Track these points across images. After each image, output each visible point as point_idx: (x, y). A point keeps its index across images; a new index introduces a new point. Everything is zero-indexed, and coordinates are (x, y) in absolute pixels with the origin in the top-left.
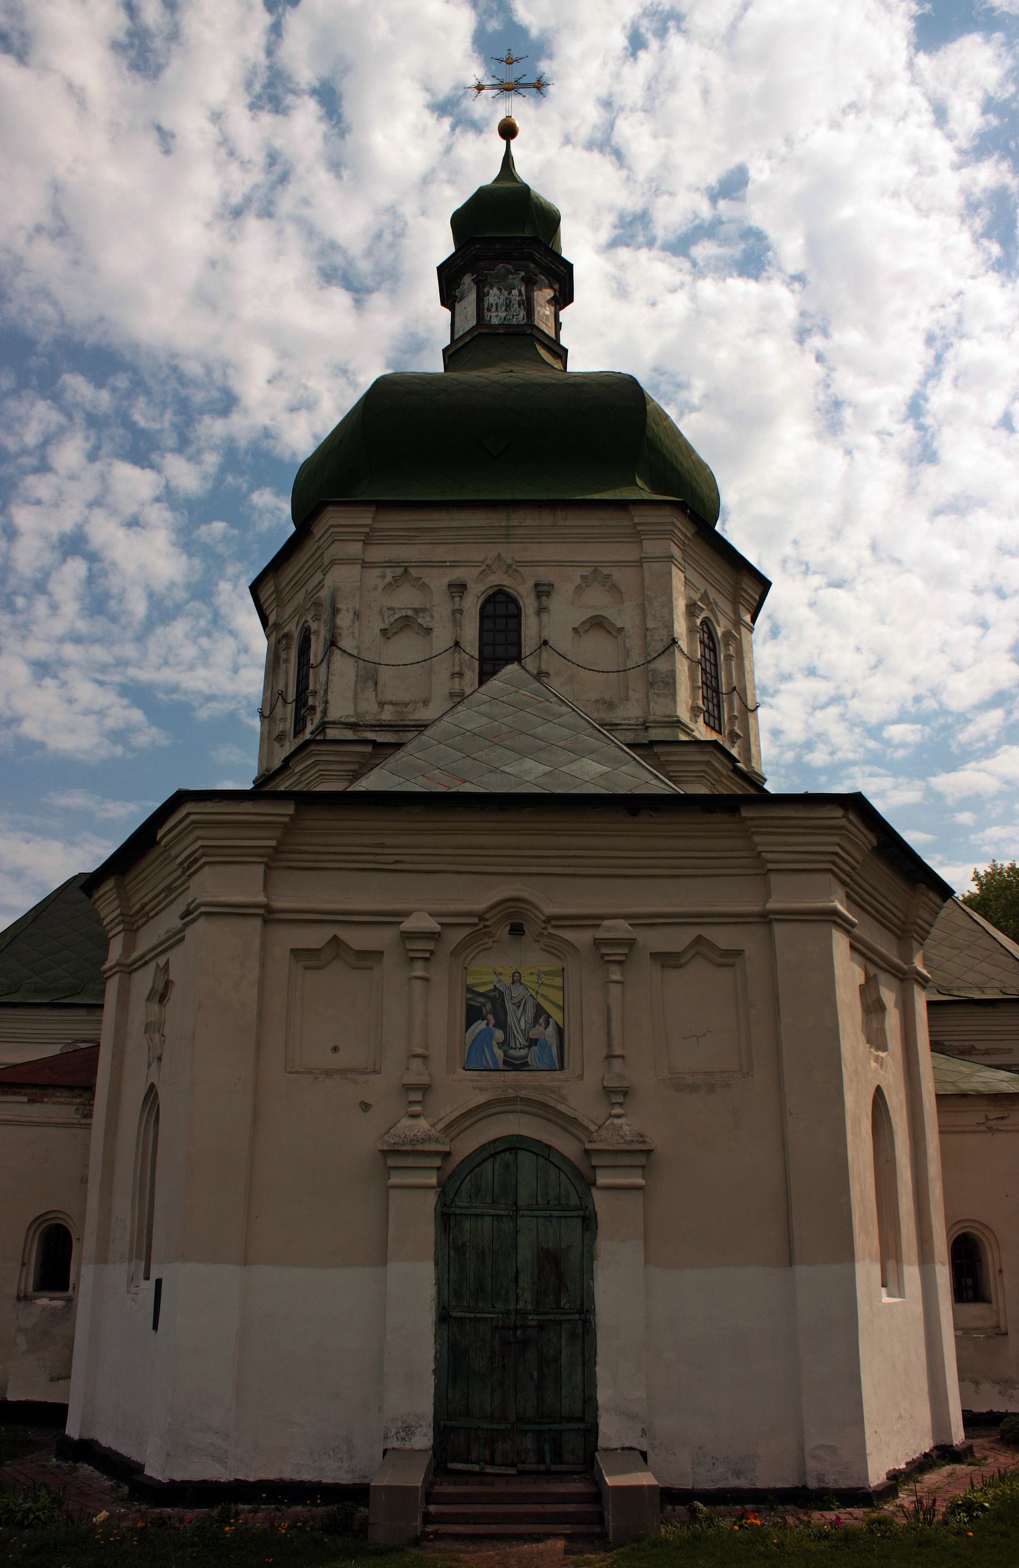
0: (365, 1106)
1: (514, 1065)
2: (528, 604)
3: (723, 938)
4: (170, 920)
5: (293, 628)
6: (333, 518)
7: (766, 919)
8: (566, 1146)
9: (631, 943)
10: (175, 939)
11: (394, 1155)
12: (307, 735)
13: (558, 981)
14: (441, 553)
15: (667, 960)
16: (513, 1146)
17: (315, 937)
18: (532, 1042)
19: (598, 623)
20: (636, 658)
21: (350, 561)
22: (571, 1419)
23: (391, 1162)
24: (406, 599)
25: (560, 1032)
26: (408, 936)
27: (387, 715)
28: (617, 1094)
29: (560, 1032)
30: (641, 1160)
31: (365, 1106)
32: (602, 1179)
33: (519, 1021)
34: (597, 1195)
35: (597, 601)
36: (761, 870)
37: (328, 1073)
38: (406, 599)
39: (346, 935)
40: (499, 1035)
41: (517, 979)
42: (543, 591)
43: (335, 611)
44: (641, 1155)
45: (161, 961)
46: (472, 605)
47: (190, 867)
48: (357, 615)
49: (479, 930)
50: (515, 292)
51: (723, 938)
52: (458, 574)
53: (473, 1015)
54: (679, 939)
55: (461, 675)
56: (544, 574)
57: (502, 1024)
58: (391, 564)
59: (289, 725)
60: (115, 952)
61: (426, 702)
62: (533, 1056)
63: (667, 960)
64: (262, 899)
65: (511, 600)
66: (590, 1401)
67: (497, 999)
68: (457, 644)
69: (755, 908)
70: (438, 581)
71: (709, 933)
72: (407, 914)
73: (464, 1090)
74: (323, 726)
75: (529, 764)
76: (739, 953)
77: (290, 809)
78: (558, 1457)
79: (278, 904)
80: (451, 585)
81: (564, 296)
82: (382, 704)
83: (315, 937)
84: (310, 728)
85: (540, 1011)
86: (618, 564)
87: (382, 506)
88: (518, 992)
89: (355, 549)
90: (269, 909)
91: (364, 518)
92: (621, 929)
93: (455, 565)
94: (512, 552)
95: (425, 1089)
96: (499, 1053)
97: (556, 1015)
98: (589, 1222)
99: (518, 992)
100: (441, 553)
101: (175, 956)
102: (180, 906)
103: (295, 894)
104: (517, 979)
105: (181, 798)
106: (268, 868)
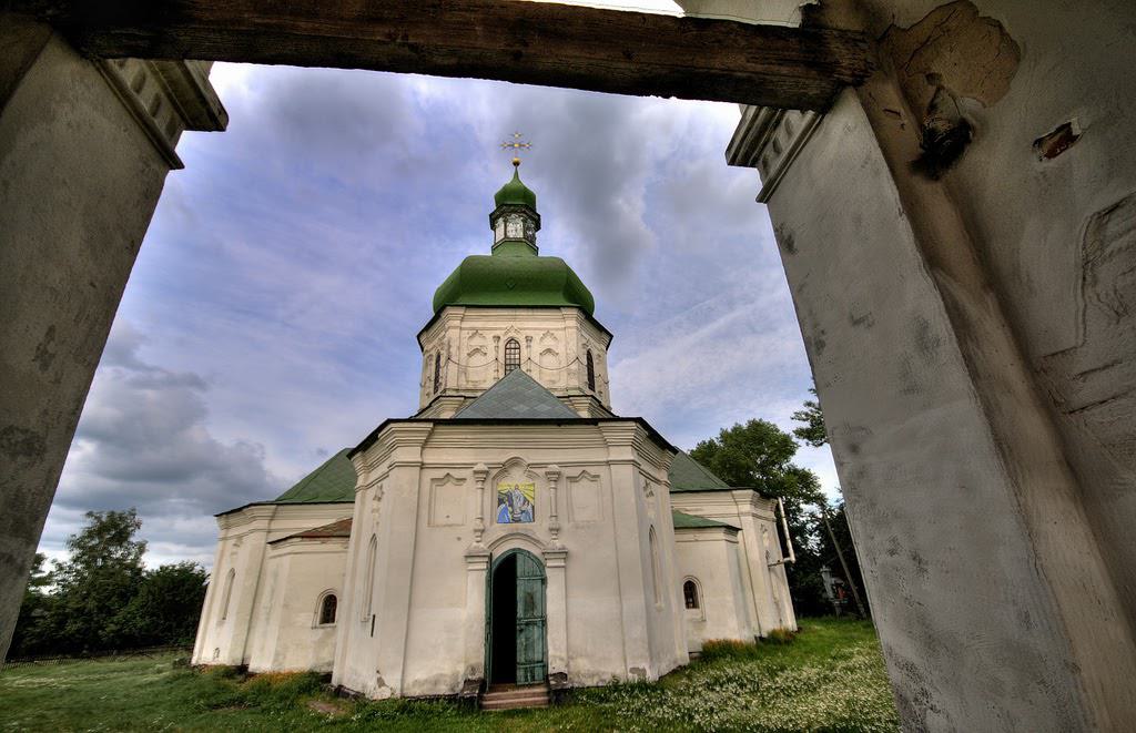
0: (459, 539)
2: (523, 344)
3: (592, 470)
4: (383, 468)
5: (434, 353)
6: (450, 311)
7: (608, 463)
8: (536, 551)
9: (559, 474)
10: (385, 476)
12: (439, 394)
13: (532, 488)
14: (491, 325)
15: (572, 479)
17: (440, 474)
18: (523, 512)
19: (549, 351)
20: (564, 364)
21: (455, 327)
22: (538, 662)
23: (469, 560)
24: (477, 342)
25: (533, 507)
26: (475, 472)
27: (470, 386)
28: (556, 531)
29: (533, 507)
30: (564, 556)
31: (459, 539)
32: (549, 563)
33: (518, 504)
34: (547, 570)
35: (549, 343)
36: (606, 445)
38: (477, 342)
39: (452, 472)
40: (510, 509)
41: (517, 488)
42: (529, 339)
43: (450, 347)
44: (564, 554)
45: (379, 484)
46: (502, 344)
47: (392, 448)
48: (459, 348)
49: (504, 468)
51: (592, 470)
52: (498, 333)
53: (501, 501)
54: (575, 472)
56: (529, 333)
57: (511, 505)
59: (432, 390)
60: (360, 482)
61: (485, 381)
62: (523, 517)
63: (572, 479)
64: (420, 460)
66: (545, 653)
69: (605, 459)
70: (490, 335)
71: (588, 469)
72: (476, 464)
73: (499, 530)
74: (445, 390)
75: (521, 406)
76: (598, 476)
77: (431, 425)
78: (533, 677)
79: (425, 461)
80: (494, 337)
81: (538, 227)
82: (468, 382)
83: (440, 474)
84: (440, 391)
85: (525, 500)
86: (557, 329)
87: (468, 307)
88: (517, 492)
89: (457, 323)
90: (423, 464)
91: (461, 311)
92: (555, 468)
94: (517, 325)
95: (483, 531)
96: (510, 516)
98: (544, 581)
99: (517, 492)
100: (491, 325)
101: (384, 482)
102: (387, 463)
103: (432, 457)
104: (517, 488)
105: (389, 421)
106: (423, 448)
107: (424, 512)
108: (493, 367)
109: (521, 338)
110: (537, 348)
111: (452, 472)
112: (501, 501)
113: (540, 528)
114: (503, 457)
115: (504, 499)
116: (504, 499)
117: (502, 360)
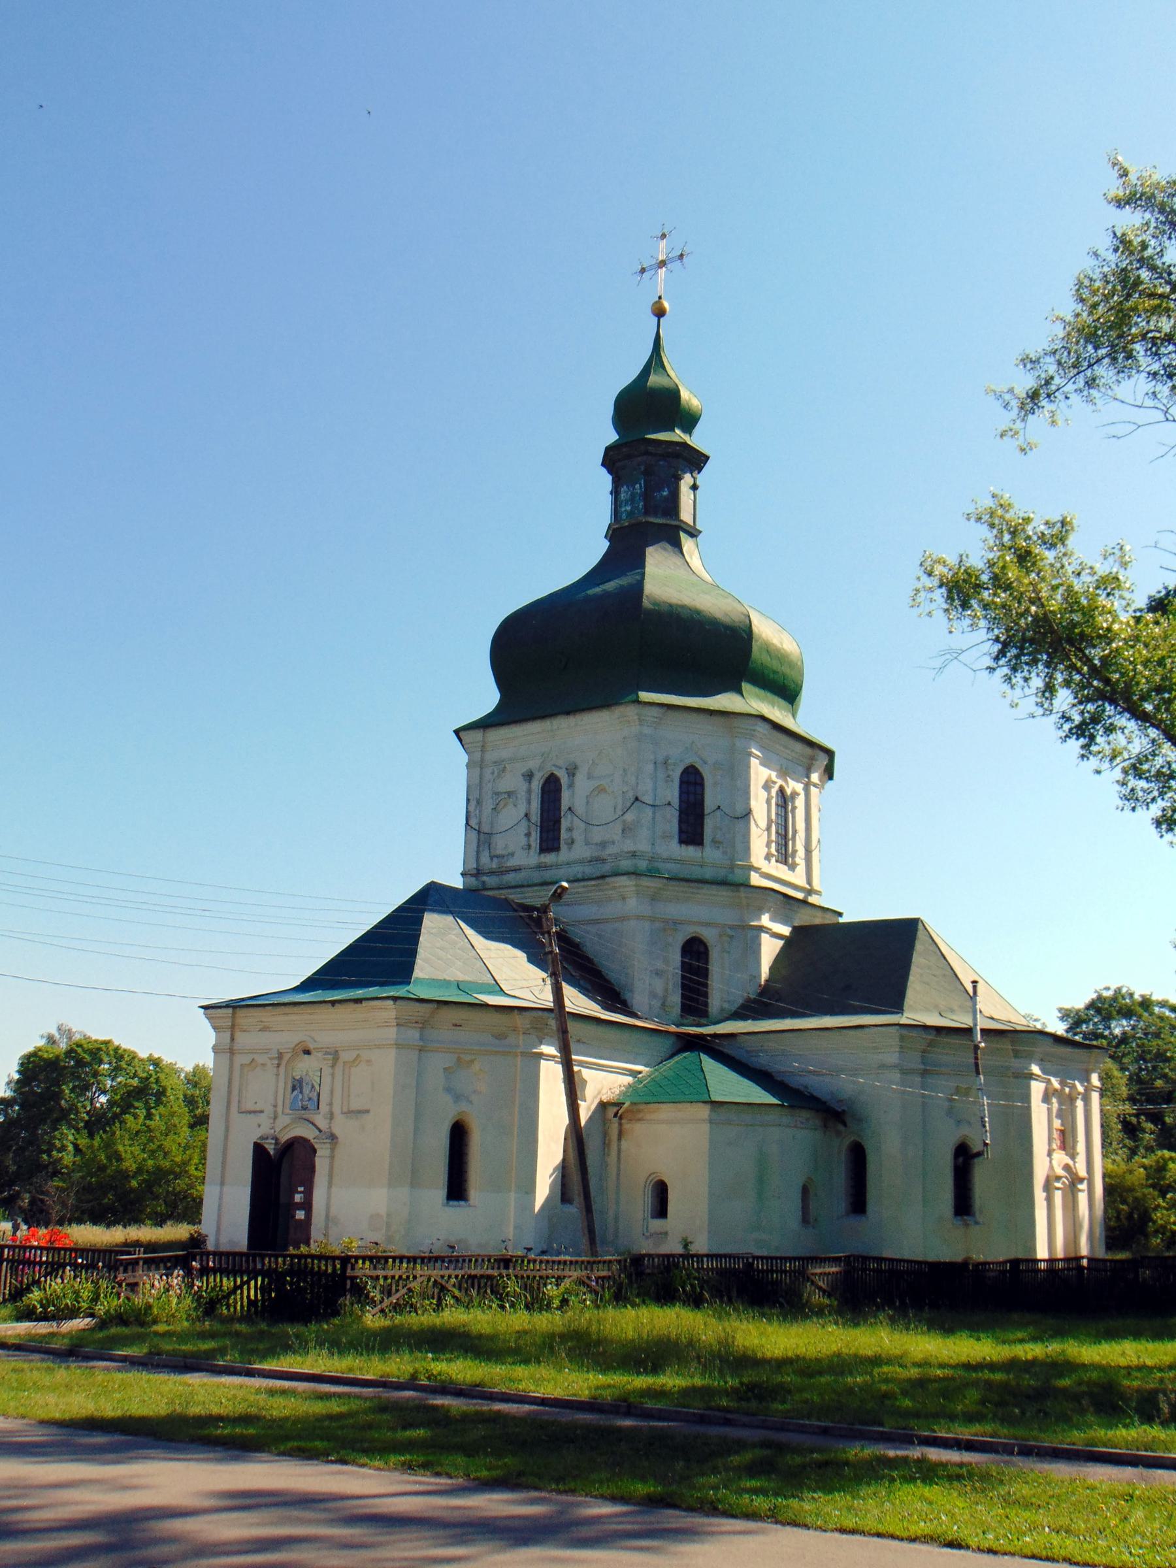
1: (305, 1108)
2: (564, 780)
18: (310, 1099)
25: (319, 1095)
33: (306, 1090)
37: (250, 1112)
42: (572, 772)
46: (537, 785)
50: (637, 486)
57: (301, 1092)
61: (512, 854)
67: (300, 1081)
68: (526, 815)
73: (283, 1121)
82: (492, 858)
97: (317, 1087)
108: (523, 828)
111: (256, 1057)
115: (297, 1085)
116: (297, 1085)
117: (536, 817)
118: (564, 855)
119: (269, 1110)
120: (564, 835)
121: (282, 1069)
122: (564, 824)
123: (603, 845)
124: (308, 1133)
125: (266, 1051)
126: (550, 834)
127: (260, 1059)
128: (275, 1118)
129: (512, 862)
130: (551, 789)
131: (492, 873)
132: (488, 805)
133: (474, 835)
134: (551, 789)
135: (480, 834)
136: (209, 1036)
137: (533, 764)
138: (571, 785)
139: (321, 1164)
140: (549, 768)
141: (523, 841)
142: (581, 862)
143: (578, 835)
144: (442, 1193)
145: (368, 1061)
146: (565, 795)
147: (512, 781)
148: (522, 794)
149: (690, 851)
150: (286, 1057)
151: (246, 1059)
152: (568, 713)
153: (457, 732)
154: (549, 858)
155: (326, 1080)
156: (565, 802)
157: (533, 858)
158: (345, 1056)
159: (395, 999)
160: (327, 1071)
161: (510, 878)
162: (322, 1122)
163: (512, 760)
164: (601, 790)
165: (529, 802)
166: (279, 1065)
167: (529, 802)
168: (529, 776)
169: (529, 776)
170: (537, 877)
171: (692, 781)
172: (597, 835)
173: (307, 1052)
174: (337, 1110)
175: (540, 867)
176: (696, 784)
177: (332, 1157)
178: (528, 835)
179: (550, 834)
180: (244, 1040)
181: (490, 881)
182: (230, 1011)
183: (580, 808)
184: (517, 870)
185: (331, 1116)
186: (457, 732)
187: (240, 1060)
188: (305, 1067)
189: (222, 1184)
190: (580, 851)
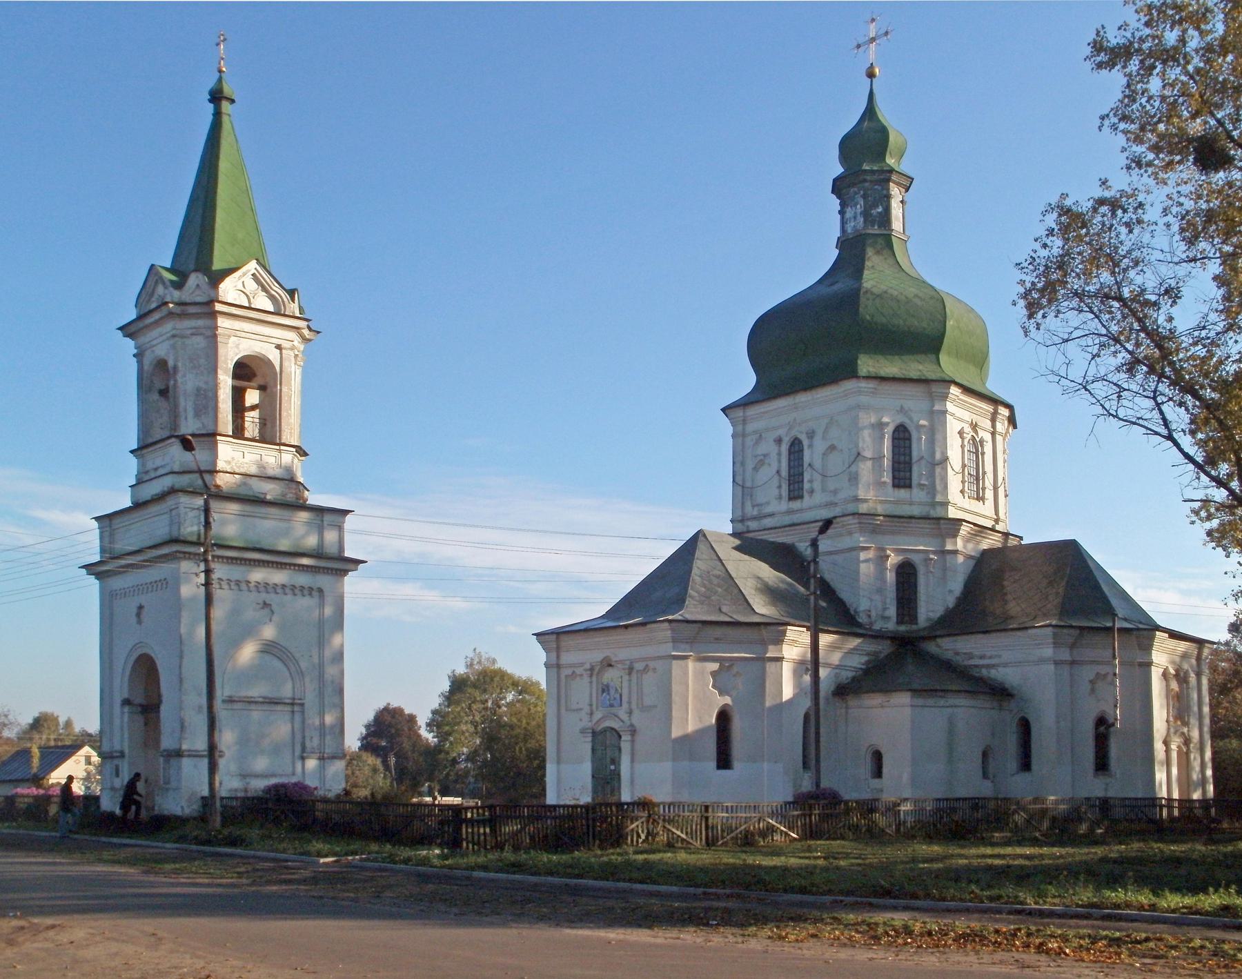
1: (612, 706)
2: (806, 443)
11: (583, 731)
16: (605, 730)
24: (763, 449)
27: (755, 513)
33: (612, 692)
38: (763, 449)
42: (811, 435)
46: (785, 448)
51: (652, 664)
53: (603, 691)
55: (780, 487)
58: (755, 432)
65: (800, 442)
67: (607, 686)
73: (598, 715)
82: (753, 506)
93: (775, 428)
98: (620, 750)
107: (563, 701)
108: (775, 482)
109: (803, 437)
110: (820, 445)
112: (603, 691)
113: (622, 713)
114: (597, 656)
116: (605, 689)
117: (784, 473)
118: (807, 501)
119: (587, 709)
120: (806, 486)
121: (594, 679)
122: (807, 477)
123: (835, 492)
124: (615, 724)
125: (582, 664)
126: (795, 488)
127: (579, 671)
128: (591, 714)
129: (768, 510)
130: (796, 449)
131: (754, 518)
132: (750, 465)
133: (740, 489)
134: (796, 449)
135: (743, 488)
136: (541, 655)
137: (781, 432)
138: (810, 446)
139: (625, 746)
140: (794, 433)
141: (776, 492)
142: (820, 506)
143: (817, 485)
144: (713, 764)
145: (654, 669)
146: (807, 453)
147: (768, 447)
148: (774, 455)
149: (903, 493)
150: (597, 669)
151: (569, 671)
152: (805, 389)
153: (724, 410)
154: (796, 505)
155: (625, 684)
156: (807, 459)
157: (784, 505)
158: (639, 666)
159: (670, 621)
160: (626, 678)
161: (768, 522)
162: (624, 717)
163: (767, 430)
164: (832, 448)
165: (779, 461)
166: (591, 676)
167: (779, 461)
168: (779, 441)
169: (779, 441)
170: (787, 520)
171: (902, 437)
172: (831, 485)
173: (610, 665)
174: (634, 706)
175: (790, 512)
176: (905, 439)
177: (633, 741)
178: (780, 487)
179: (795, 488)
180: (566, 658)
181: (753, 525)
182: (554, 637)
183: (818, 464)
184: (771, 515)
185: (630, 713)
186: (724, 410)
187: (565, 672)
188: (610, 676)
189: (559, 762)
190: (819, 498)
